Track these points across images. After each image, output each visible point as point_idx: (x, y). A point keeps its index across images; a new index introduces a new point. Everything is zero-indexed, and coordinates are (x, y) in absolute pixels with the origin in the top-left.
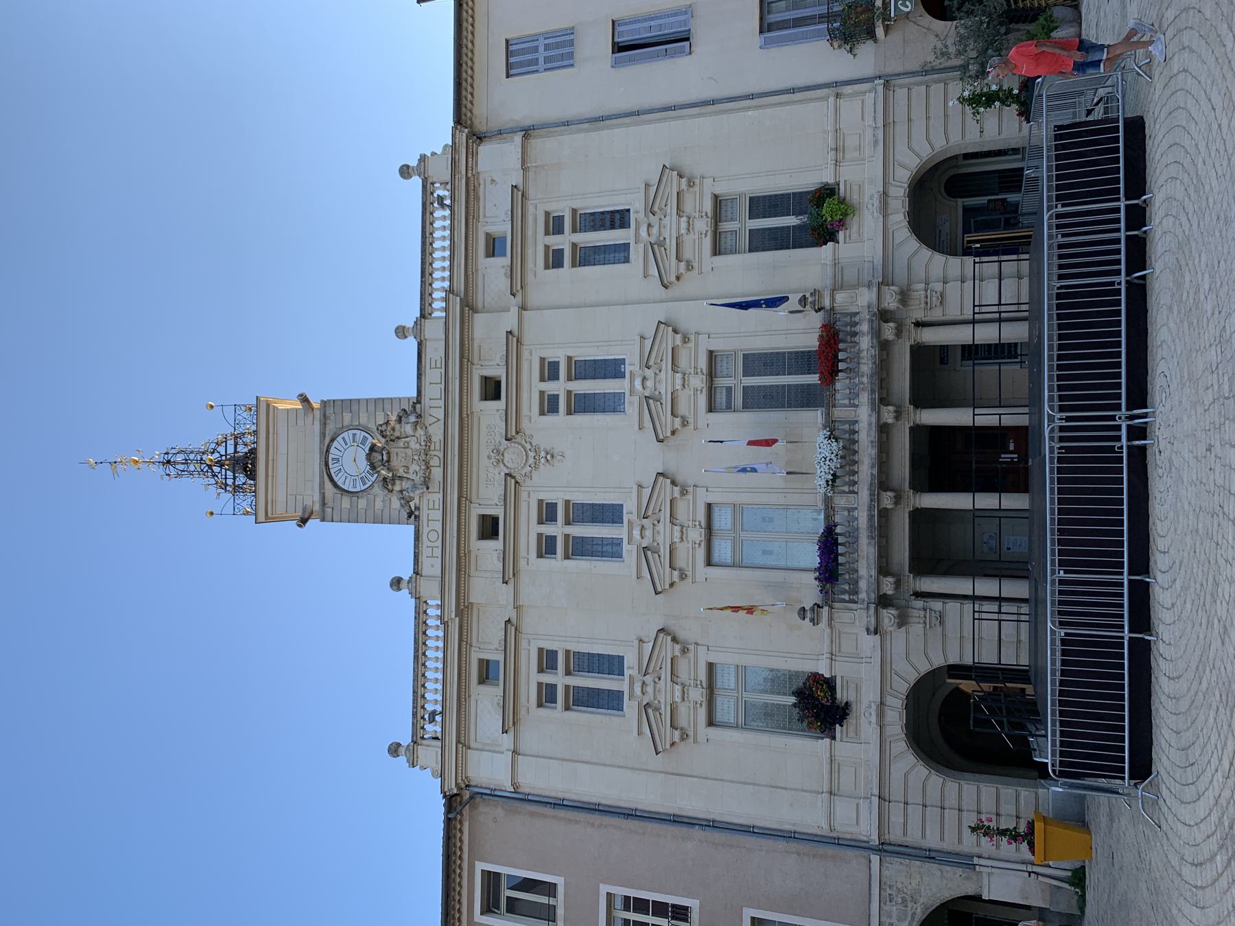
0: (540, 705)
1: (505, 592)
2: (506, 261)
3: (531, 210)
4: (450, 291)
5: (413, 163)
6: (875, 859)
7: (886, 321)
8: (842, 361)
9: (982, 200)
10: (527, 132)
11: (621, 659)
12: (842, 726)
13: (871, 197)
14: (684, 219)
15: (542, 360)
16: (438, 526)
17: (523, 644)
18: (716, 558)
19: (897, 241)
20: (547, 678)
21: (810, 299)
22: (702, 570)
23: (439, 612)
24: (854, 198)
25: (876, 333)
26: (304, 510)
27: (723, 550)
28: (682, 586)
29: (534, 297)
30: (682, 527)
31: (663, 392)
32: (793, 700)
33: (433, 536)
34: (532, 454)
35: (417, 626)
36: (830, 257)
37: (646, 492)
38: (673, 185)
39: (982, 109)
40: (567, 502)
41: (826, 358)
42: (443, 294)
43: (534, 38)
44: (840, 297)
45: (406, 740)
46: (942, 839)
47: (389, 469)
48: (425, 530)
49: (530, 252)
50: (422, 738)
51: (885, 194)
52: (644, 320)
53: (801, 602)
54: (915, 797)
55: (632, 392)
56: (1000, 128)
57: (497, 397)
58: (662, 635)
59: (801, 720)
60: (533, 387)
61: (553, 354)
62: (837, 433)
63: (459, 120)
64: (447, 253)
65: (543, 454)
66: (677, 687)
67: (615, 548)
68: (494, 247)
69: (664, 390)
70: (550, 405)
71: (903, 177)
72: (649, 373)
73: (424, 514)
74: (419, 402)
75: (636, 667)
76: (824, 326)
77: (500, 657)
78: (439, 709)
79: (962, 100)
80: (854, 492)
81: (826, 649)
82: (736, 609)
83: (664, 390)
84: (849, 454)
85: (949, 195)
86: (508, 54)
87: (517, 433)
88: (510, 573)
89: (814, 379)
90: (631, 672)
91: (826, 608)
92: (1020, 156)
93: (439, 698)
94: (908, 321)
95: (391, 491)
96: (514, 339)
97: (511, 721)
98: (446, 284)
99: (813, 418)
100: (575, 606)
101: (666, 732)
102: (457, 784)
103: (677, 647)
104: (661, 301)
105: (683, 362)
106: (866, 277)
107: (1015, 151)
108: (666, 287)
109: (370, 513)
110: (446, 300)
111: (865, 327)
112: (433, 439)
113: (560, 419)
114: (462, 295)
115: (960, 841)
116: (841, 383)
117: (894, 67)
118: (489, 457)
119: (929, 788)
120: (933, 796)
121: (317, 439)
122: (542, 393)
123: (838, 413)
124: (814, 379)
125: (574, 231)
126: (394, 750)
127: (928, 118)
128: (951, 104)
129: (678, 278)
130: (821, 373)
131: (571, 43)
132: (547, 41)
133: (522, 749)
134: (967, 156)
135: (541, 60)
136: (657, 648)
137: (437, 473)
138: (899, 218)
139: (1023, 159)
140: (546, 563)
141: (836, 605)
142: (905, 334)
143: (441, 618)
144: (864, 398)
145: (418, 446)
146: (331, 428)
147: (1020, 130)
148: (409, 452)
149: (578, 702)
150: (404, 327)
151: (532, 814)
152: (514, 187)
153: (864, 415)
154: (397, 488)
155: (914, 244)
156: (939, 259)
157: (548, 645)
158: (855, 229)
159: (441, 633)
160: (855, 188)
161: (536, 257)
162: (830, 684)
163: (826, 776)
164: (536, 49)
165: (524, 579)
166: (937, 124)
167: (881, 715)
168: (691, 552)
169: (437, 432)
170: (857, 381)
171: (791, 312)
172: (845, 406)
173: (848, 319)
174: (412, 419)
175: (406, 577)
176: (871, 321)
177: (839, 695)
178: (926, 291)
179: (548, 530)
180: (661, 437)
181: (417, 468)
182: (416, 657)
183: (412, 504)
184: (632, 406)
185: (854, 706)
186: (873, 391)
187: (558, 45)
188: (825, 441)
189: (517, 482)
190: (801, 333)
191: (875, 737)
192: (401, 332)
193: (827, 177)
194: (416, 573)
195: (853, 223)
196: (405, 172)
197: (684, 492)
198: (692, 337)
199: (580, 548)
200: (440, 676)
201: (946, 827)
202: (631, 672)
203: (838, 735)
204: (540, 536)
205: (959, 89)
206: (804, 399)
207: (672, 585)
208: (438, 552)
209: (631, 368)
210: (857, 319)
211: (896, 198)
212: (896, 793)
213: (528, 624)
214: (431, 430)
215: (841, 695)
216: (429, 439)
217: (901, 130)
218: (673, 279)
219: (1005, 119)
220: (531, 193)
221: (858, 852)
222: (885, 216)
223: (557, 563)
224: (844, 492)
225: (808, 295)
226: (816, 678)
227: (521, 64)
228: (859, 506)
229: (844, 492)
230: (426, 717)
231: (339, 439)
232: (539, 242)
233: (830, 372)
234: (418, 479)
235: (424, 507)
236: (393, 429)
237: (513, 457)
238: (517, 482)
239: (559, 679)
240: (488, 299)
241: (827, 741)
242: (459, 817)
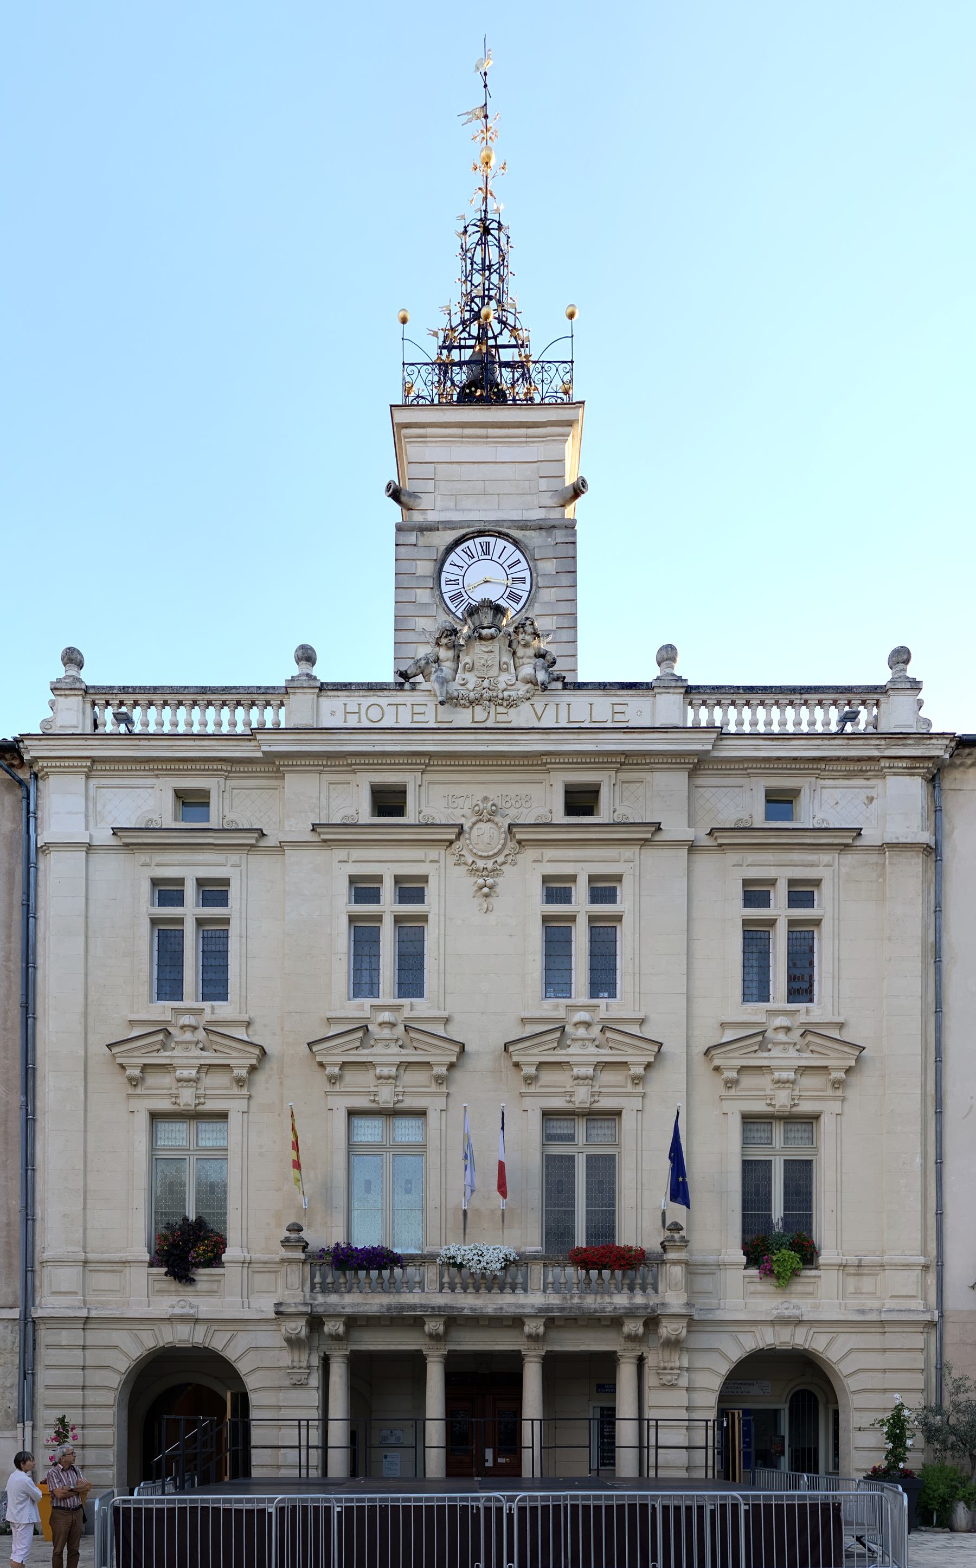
0: (155, 882)
1: (299, 829)
2: (759, 820)
3: (825, 857)
4: (722, 734)
5: (912, 671)
6: (15, 1313)
7: (646, 1325)
8: (600, 1273)
9: (785, 1430)
10: (933, 852)
11: (224, 997)
12: (166, 1274)
13: (797, 1307)
14: (792, 1075)
15: (618, 878)
16: (388, 722)
17: (234, 857)
18: (358, 1122)
19: (741, 1337)
20: (190, 891)
21: (676, 1236)
22: (342, 1104)
23: (269, 725)
24: (798, 1287)
25: (631, 1313)
26: (414, 495)
27: (369, 1131)
28: (319, 1079)
29: (706, 864)
30: (396, 1078)
31: (570, 1051)
32: (192, 1217)
33: (375, 713)
34: (490, 865)
35: (248, 690)
36: (727, 1259)
37: (439, 1030)
38: (837, 1061)
39: (885, 1429)
40: (424, 918)
41: (603, 1255)
42: (718, 724)
44: (677, 1272)
45: (90, 676)
46: (48, 1387)
48: (383, 700)
49: (769, 857)
50: (94, 704)
51: (799, 1322)
52: (665, 1026)
53: (309, 1226)
54: (92, 1357)
55: (571, 1008)
56: (863, 1446)
57: (571, 809)
58: (257, 1051)
59: (169, 1226)
60: (581, 864)
61: (625, 892)
62: (513, 1269)
64: (776, 729)
65: (490, 881)
66: (194, 1072)
67: (366, 988)
68: (781, 801)
69: (573, 1052)
70: (557, 890)
71: (818, 1343)
72: (595, 1031)
73: (405, 698)
74: (565, 686)
75: (214, 1018)
76: (642, 1252)
77: (214, 823)
78: (137, 729)
79: (899, 1408)
80: (442, 1287)
81: (257, 1256)
82: (296, 1146)
83: (573, 1052)
84: (487, 1282)
85: (795, 1394)
87: (519, 842)
88: (328, 835)
89: (581, 1241)
90: (208, 1010)
91: (302, 1256)
92: (831, 1470)
93: (152, 729)
94: (644, 1349)
95: (438, 644)
97: (131, 840)
98: (732, 728)
99: (533, 1243)
100: (288, 927)
101: (137, 1058)
102: (36, 759)
103: (244, 1073)
104: (688, 1046)
105: (608, 1077)
106: (700, 1302)
107: (836, 1466)
108: (707, 1052)
109: (409, 610)
110: (711, 727)
111: (639, 1299)
112: (512, 711)
113: (538, 907)
114: (715, 754)
115: (48, 1406)
116: (572, 1273)
117: (952, 1332)
118: (486, 799)
119: (104, 1372)
120: (96, 1378)
121: (516, 516)
122: (573, 878)
123: (537, 1270)
124: (581, 1241)
125: (792, 923)
126: (72, 658)
127: (884, 1371)
128: (897, 1395)
129: (717, 1069)
130: (585, 1250)
134: (836, 1413)
136: (240, 1046)
137: (463, 717)
138: (768, 1338)
139: (827, 1473)
140: (343, 887)
141: (307, 1268)
142: (630, 1345)
143: (262, 729)
144: (554, 1300)
145: (502, 686)
146: (533, 539)
147: (858, 1470)
148: (494, 672)
150: (674, 659)
151: (10, 874)
152: (858, 832)
153: (533, 1300)
154: (444, 653)
155: (736, 1355)
156: (716, 1383)
157: (234, 892)
158: (760, 1287)
159: (240, 729)
160: (810, 1289)
161: (761, 866)
162: (214, 1260)
163: (106, 1257)
165: (319, 857)
166: (876, 1381)
167: (184, 1319)
168: (362, 1089)
169: (521, 716)
170: (575, 1291)
171: (664, 1214)
172: (545, 1278)
173: (650, 1280)
174: (541, 676)
175: (316, 671)
176: (646, 1307)
177: (202, 1271)
178: (680, 1368)
179: (388, 890)
180: (511, 1049)
181: (470, 686)
182: (204, 690)
183: (420, 678)
184: (553, 1008)
185: (190, 1288)
186: (562, 1309)
188: (501, 1255)
189: (451, 842)
190: (637, 1227)
191: (157, 1312)
192: (667, 655)
193: (825, 1256)
194: (323, 688)
195: (767, 1286)
196: (901, 657)
197: (439, 1080)
198: (640, 1089)
199: (364, 936)
200: (181, 729)
201: (63, 1392)
202: (208, 1010)
203: (155, 1270)
205: (914, 1404)
206: (557, 1231)
207: (321, 1065)
208: (352, 722)
209: (603, 1007)
210: (650, 1291)
211: (793, 1335)
212: (95, 1337)
213: (260, 864)
214: (525, 707)
215: (202, 1274)
216: (512, 704)
217: (874, 1340)
218: (717, 1062)
219: (872, 1454)
220: (849, 859)
221: (20, 1292)
222: (772, 1323)
223: (343, 905)
224: (442, 1276)
225: (683, 1233)
226: (221, 1244)
228: (426, 1294)
229: (442, 1276)
230: (124, 709)
232: (780, 869)
233: (584, 1260)
234: (455, 687)
236: (526, 645)
237: (485, 837)
238: (451, 842)
239: (190, 909)
240: (707, 793)
241: (147, 1258)
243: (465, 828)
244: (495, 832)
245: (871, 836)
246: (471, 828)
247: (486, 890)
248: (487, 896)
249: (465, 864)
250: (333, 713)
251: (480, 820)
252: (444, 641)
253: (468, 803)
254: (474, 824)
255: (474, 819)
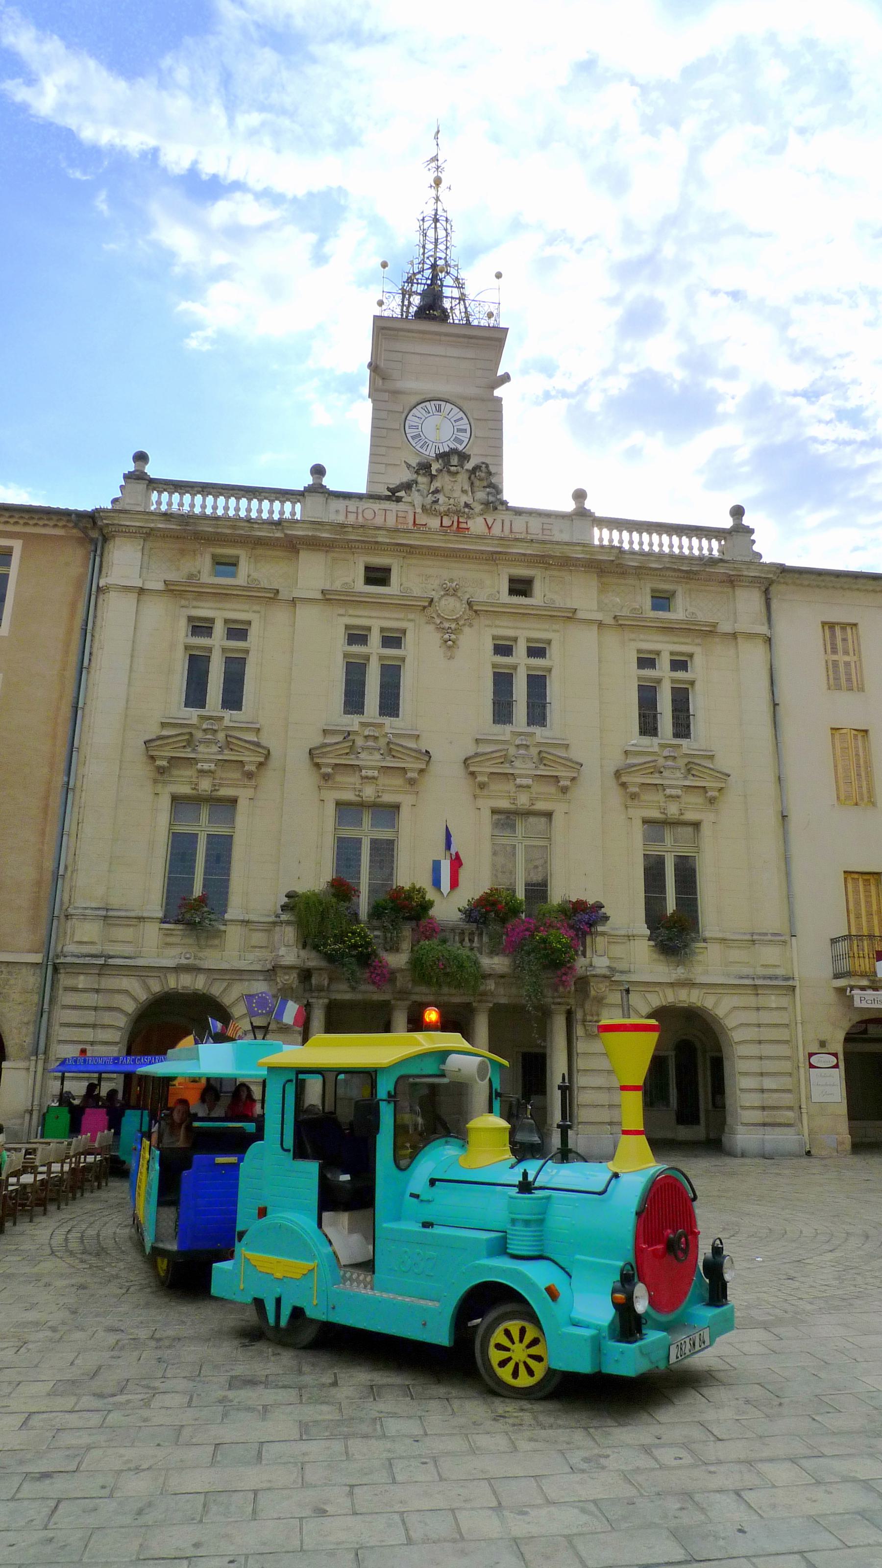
0: (190, 619)
5: (746, 521)
10: (769, 641)
19: (648, 995)
34: (453, 626)
43: (857, 652)
47: (439, 471)
63: (783, 570)
65: (453, 637)
86: (844, 626)
87: (476, 611)
96: (570, 616)
113: (489, 657)
122: (515, 640)
127: (759, 1026)
131: (851, 689)
132: (853, 665)
133: (145, 598)
135: (835, 657)
149: (193, 659)
164: (846, 653)
187: (848, 674)
196: (738, 512)
197: (412, 782)
204: (369, 629)
227: (833, 636)
231: (461, 414)
235: (401, 506)
238: (425, 607)
239: (218, 640)
242: (71, 525)
243: (435, 600)
244: (458, 605)
245: (725, 627)
246: (440, 599)
247: (450, 643)
248: (450, 647)
249: (434, 623)
250: (337, 511)
251: (447, 594)
252: (421, 472)
253: (437, 582)
254: (442, 596)
255: (442, 593)
